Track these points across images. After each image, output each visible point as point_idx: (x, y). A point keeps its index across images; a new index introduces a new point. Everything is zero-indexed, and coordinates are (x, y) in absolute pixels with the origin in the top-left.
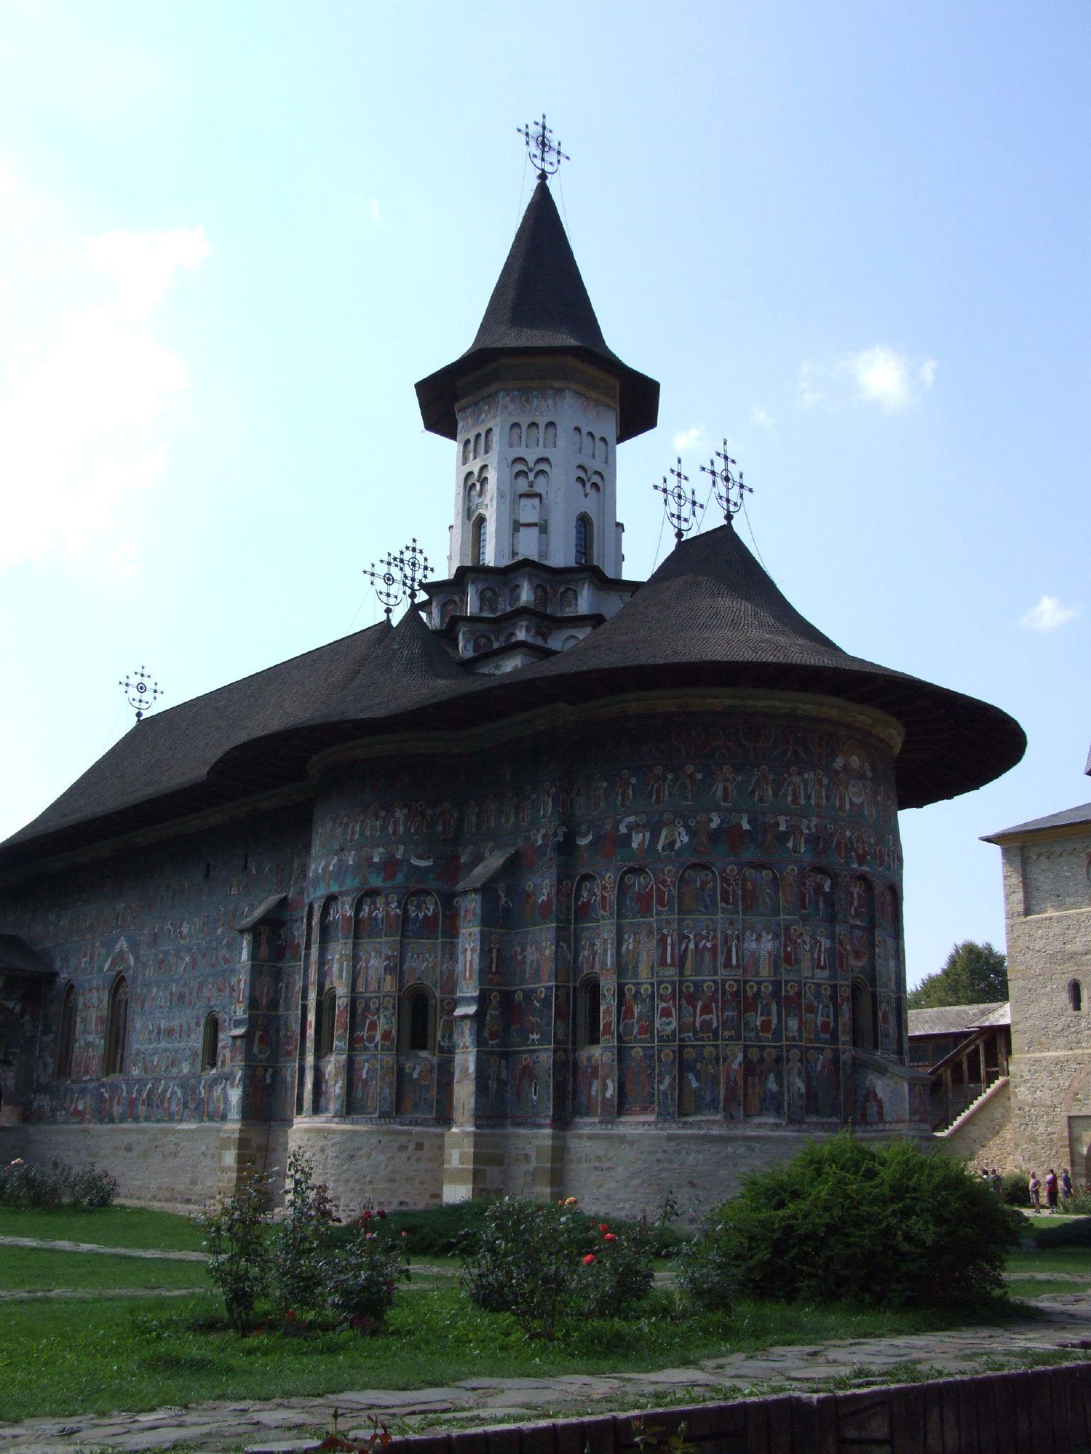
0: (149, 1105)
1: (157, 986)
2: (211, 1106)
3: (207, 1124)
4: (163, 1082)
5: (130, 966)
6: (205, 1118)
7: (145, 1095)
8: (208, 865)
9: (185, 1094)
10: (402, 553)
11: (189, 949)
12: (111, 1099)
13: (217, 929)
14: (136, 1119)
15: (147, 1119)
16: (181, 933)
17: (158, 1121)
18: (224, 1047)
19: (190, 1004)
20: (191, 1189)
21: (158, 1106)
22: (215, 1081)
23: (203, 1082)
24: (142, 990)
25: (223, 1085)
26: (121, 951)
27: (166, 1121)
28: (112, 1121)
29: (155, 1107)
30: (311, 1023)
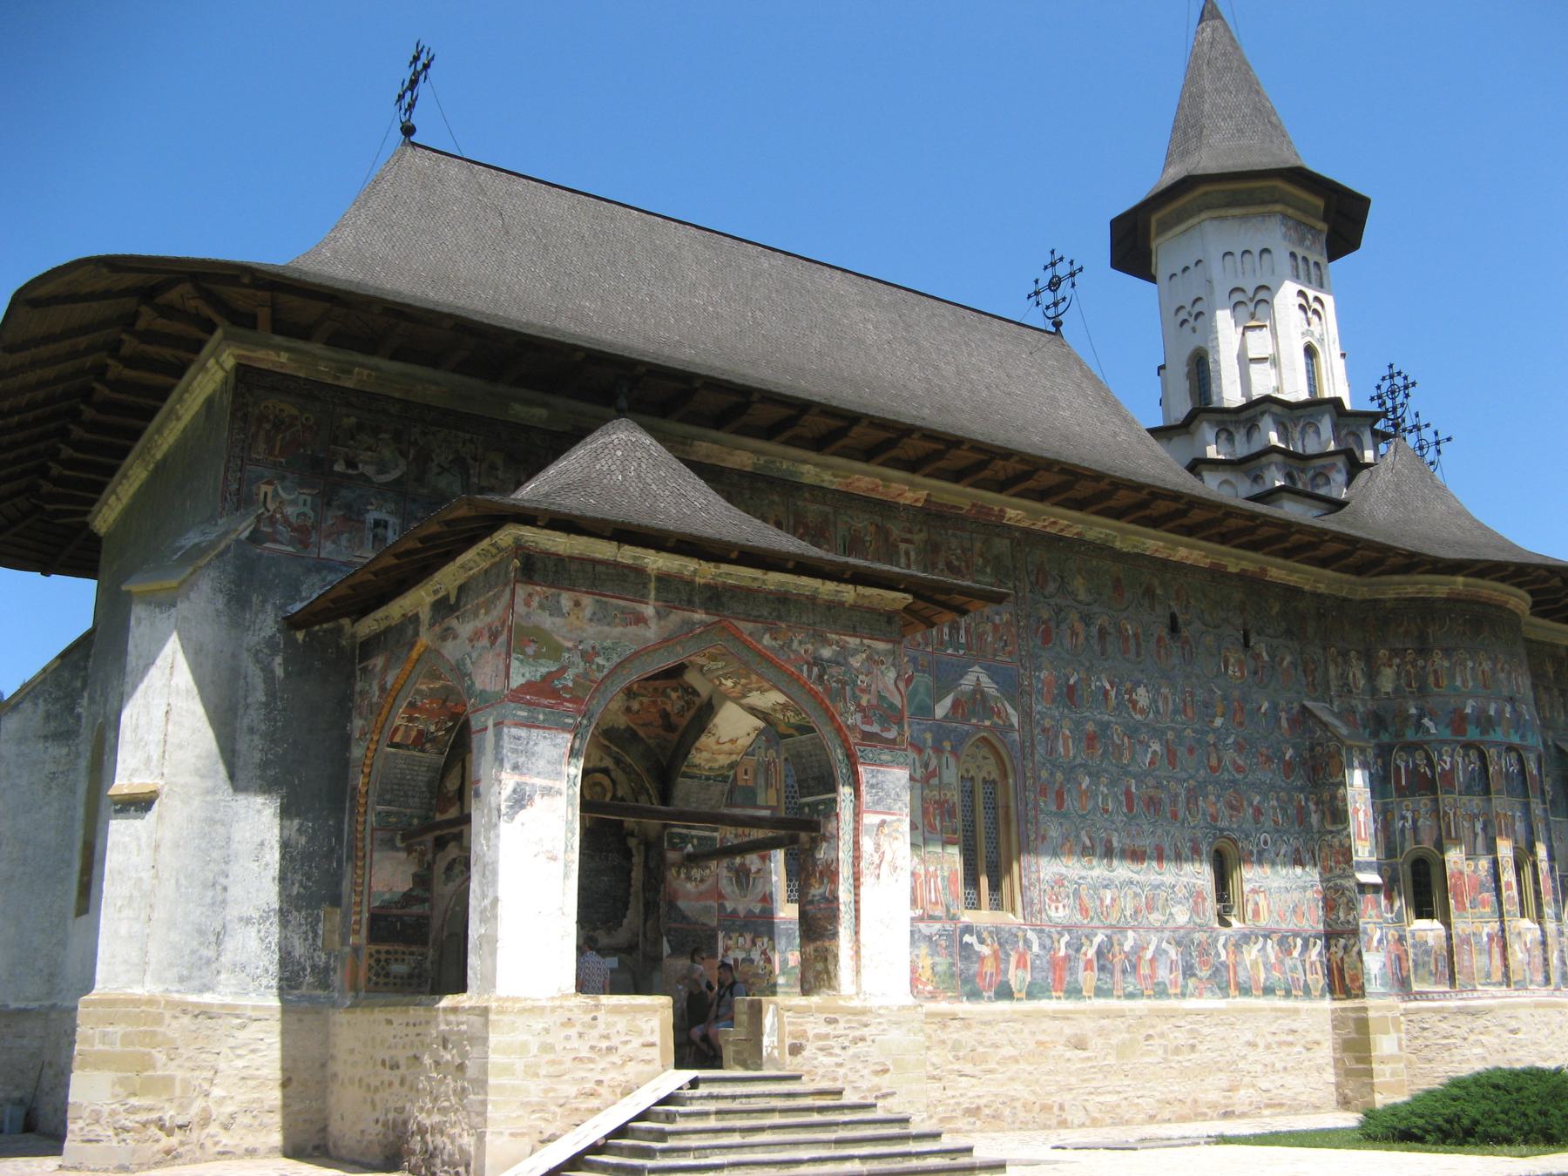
0: (1102, 968)
1: (1090, 774)
2: (1242, 977)
3: (1238, 999)
4: (1130, 934)
5: (1012, 726)
6: (1232, 991)
7: (1091, 952)
8: (1173, 618)
9: (1186, 953)
10: (1399, 373)
11: (1158, 734)
12: (1000, 958)
13: (1215, 716)
14: (1075, 992)
15: (1100, 992)
16: (1134, 703)
17: (1130, 996)
18: (1254, 891)
19: (1175, 815)
20: (1230, 1097)
21: (1124, 972)
22: (1246, 938)
23: (1222, 940)
24: (1052, 774)
25: (1259, 945)
26: (978, 689)
27: (1149, 997)
28: (1005, 993)
29: (1118, 975)
30: (1509, 885)
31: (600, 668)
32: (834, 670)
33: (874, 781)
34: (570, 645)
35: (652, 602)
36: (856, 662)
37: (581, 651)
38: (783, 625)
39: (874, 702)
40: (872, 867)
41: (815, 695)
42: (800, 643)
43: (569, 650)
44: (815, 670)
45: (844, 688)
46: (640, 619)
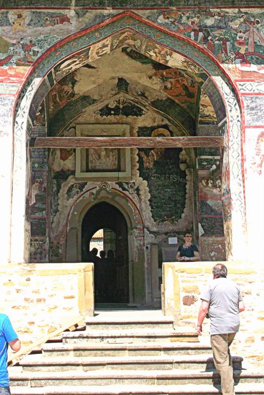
31: (35, 53)
32: (217, 33)
33: (253, 105)
34: (14, 42)
35: (73, 8)
36: (235, 25)
37: (23, 45)
38: (174, 8)
39: (251, 50)
40: (254, 167)
41: (202, 50)
42: (188, 18)
43: (14, 45)
44: (201, 34)
45: (224, 44)
46: (64, 19)
